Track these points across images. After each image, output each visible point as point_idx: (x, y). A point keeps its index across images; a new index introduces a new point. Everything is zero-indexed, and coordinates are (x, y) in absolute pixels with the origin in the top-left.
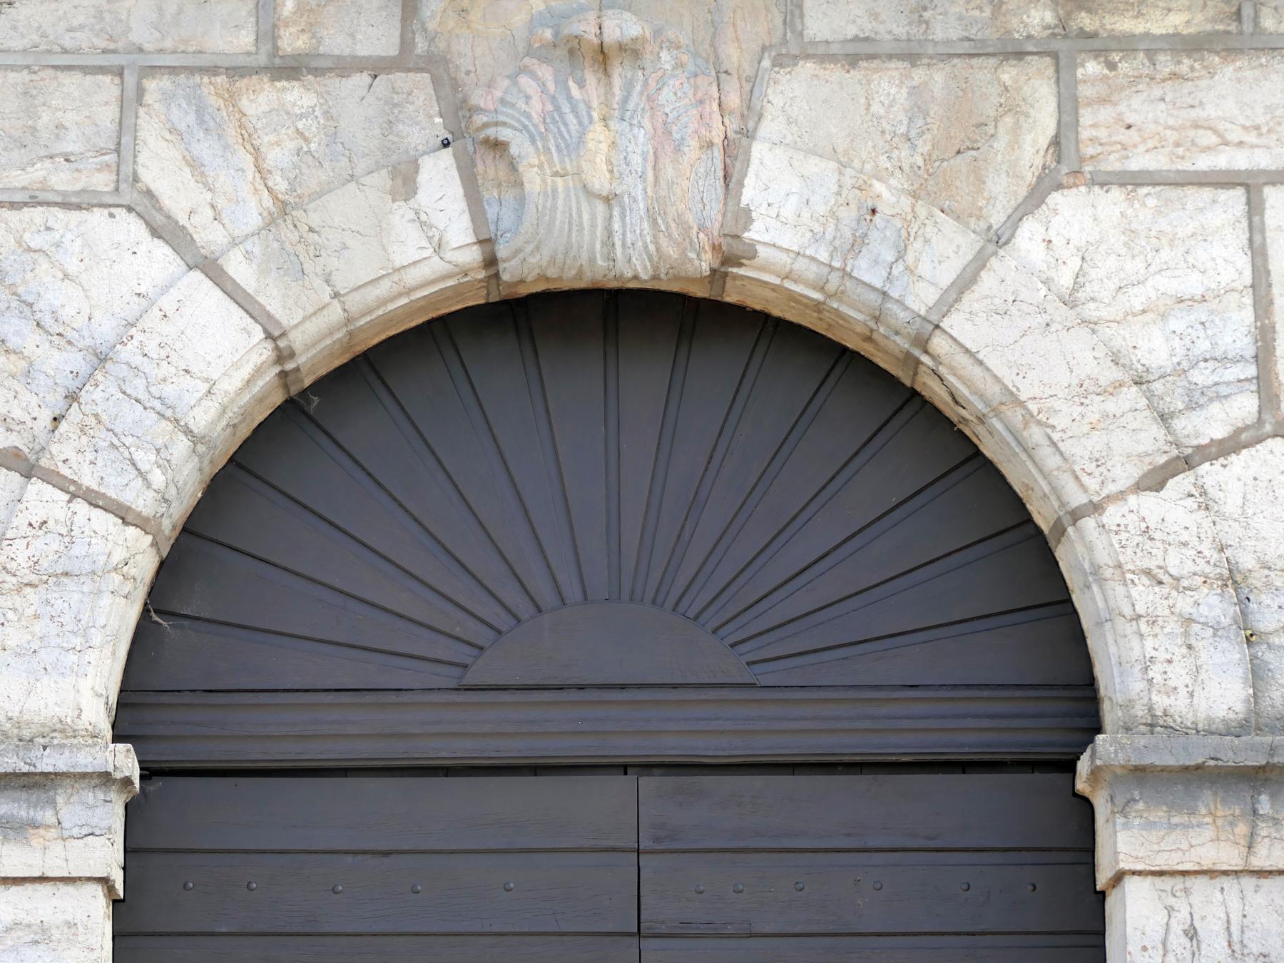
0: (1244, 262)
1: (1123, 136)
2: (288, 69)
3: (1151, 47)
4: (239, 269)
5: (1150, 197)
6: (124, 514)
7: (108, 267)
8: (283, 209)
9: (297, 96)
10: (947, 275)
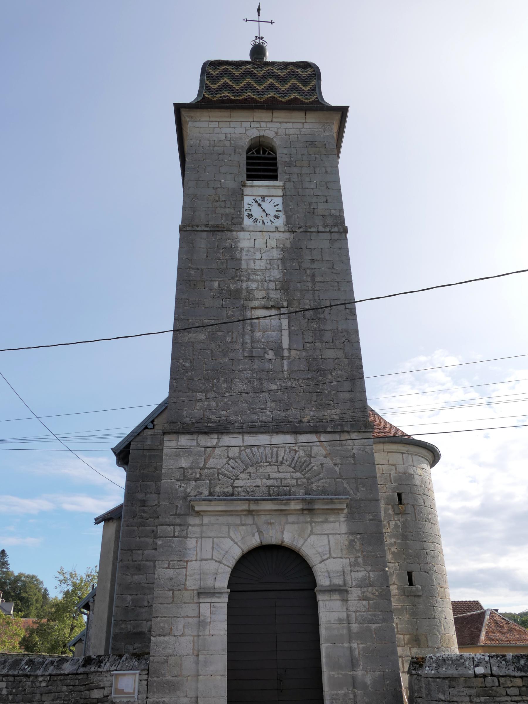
2: (243, 525)
3: (319, 522)
4: (239, 544)
6: (229, 567)
7: (227, 544)
8: (243, 538)
9: (244, 527)
10: (302, 544)
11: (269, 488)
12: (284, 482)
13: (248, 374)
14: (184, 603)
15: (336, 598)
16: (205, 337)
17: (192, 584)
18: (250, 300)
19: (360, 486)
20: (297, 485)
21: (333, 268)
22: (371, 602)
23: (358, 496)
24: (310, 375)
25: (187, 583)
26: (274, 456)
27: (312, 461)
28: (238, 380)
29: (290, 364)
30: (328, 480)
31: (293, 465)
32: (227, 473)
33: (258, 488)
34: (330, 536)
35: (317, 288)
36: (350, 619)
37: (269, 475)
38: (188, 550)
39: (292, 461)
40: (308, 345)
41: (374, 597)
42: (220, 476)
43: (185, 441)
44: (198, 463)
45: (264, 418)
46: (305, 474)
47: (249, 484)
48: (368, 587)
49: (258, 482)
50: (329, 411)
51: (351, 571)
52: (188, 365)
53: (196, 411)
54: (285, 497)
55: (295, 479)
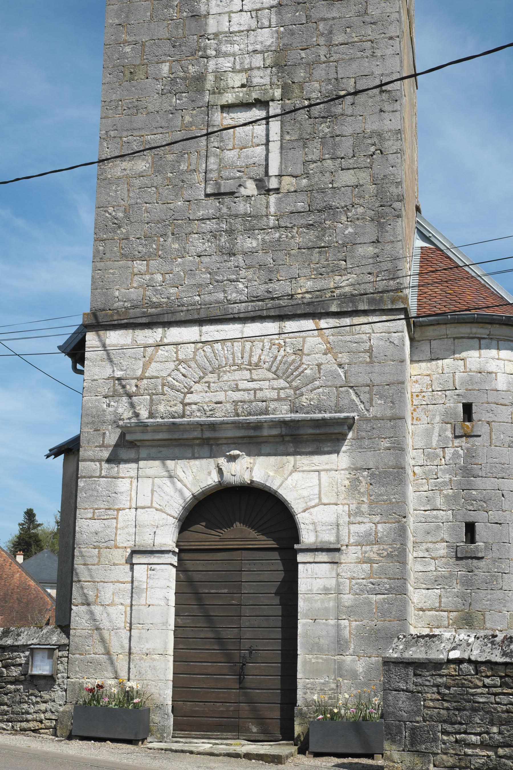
0: (318, 481)
1: (302, 465)
5: (306, 473)
10: (278, 484)
11: (236, 405)
12: (259, 394)
13: (210, 225)
14: (114, 564)
15: (322, 560)
16: (147, 165)
17: (126, 540)
18: (219, 93)
19: (375, 398)
20: (279, 399)
21: (366, 13)
22: (375, 565)
23: (373, 412)
24: (311, 219)
25: (118, 538)
26: (246, 355)
27: (304, 361)
28: (196, 236)
29: (279, 201)
30: (327, 390)
31: (274, 369)
32: (176, 383)
33: (219, 405)
34: (322, 473)
35: (336, 57)
36: (341, 587)
37: (237, 385)
38: (119, 495)
39: (273, 362)
40: (312, 166)
41: (381, 559)
42: (166, 388)
43: (115, 338)
44: (134, 370)
45: (234, 295)
46: (293, 380)
47: (207, 400)
48: (373, 544)
49: (221, 396)
50: (337, 278)
51: (350, 523)
52: (120, 215)
53: (132, 290)
54: (259, 417)
55: (275, 389)
